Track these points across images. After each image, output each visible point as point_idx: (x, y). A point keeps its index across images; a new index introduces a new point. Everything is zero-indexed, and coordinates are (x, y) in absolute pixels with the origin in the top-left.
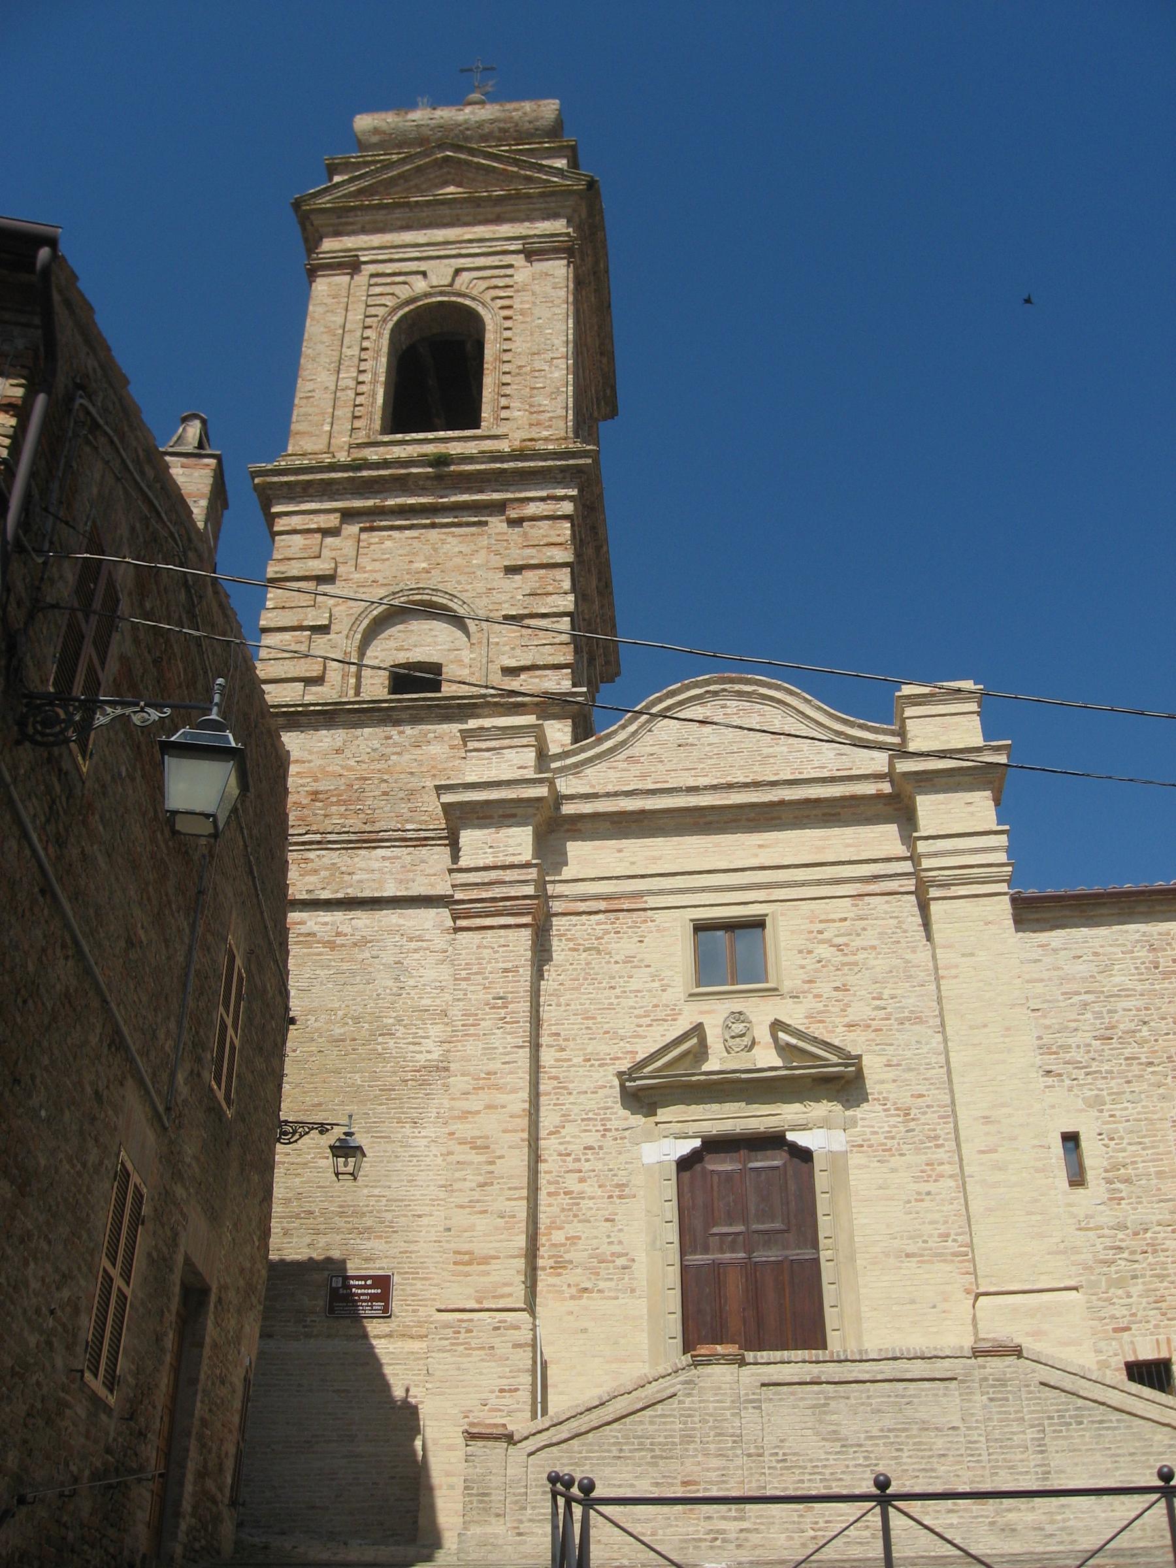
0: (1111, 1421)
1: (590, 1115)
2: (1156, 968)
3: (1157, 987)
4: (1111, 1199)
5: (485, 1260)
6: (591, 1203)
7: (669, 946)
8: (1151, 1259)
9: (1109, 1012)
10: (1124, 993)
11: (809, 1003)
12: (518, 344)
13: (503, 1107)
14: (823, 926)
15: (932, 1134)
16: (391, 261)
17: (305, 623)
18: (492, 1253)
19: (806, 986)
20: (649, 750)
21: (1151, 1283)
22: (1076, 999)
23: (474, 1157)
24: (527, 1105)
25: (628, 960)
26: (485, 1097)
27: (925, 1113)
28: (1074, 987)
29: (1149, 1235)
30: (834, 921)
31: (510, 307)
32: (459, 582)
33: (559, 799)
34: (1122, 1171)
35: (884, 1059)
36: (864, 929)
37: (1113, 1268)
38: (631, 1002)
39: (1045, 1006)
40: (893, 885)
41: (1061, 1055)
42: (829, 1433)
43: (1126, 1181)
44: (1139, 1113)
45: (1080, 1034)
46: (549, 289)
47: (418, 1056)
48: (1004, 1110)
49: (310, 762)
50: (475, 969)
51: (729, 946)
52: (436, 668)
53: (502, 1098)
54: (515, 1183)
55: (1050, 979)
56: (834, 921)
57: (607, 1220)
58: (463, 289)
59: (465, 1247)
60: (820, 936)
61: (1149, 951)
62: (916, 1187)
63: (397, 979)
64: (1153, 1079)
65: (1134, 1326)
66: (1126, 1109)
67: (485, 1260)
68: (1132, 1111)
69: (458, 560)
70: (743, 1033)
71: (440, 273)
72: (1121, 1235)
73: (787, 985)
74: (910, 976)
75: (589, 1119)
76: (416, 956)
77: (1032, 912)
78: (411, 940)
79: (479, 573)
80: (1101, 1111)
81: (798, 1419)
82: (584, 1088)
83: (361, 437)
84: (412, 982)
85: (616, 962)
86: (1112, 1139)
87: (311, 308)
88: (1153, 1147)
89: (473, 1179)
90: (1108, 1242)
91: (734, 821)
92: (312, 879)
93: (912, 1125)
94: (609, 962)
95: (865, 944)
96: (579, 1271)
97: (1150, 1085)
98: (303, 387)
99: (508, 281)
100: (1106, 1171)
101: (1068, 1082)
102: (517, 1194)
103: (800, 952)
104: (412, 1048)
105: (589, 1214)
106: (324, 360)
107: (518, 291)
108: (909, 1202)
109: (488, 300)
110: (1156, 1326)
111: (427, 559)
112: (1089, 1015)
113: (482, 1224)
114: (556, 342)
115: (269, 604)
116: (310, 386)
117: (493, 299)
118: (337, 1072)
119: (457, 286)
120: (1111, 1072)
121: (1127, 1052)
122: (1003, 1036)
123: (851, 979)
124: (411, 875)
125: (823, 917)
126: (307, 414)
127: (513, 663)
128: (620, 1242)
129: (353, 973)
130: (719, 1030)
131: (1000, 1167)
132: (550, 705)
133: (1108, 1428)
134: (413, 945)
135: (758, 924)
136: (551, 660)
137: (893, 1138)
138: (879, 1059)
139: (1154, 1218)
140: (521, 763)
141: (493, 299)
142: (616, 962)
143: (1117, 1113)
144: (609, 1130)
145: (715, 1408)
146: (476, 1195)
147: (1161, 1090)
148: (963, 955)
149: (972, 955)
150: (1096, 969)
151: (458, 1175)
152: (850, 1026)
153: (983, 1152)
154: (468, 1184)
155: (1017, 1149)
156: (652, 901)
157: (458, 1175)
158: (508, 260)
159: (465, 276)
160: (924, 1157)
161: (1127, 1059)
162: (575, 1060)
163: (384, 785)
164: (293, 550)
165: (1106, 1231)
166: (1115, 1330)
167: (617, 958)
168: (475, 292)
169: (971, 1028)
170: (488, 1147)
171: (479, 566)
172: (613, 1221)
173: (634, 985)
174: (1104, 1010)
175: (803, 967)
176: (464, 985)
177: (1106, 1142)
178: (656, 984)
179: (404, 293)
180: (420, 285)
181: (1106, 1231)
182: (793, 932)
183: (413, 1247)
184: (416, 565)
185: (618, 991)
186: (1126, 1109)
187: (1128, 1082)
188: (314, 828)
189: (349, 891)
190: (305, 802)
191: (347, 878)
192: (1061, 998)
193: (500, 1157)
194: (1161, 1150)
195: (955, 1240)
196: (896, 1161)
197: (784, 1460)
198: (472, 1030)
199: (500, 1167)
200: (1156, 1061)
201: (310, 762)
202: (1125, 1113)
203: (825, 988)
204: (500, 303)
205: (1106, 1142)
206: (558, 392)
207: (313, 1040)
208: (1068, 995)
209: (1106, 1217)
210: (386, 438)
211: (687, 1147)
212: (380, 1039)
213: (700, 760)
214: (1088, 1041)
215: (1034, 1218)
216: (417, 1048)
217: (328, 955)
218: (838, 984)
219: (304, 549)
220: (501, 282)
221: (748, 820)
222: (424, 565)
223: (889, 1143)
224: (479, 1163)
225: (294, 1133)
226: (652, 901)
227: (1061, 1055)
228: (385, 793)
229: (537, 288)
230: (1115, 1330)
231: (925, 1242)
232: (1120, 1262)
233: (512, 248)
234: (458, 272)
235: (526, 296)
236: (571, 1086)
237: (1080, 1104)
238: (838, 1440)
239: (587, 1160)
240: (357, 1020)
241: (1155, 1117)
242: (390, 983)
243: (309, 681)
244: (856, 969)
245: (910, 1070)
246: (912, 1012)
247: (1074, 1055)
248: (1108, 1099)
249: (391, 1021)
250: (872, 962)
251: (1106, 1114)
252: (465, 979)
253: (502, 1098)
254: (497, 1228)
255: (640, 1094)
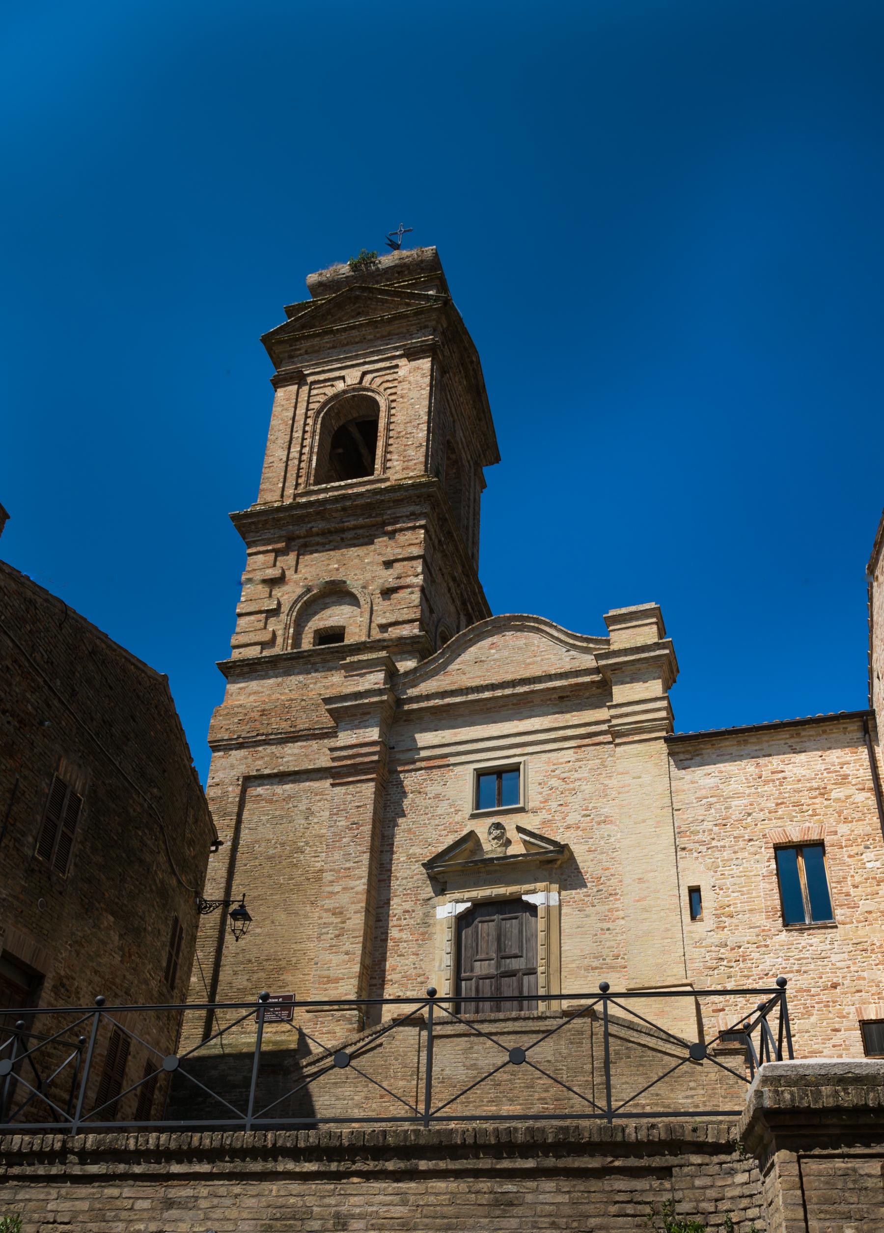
0: (649, 1056)
1: (409, 892)
2: (760, 778)
3: (759, 790)
4: (718, 928)
5: (337, 980)
6: (405, 945)
7: (460, 785)
8: (742, 965)
9: (726, 808)
10: (737, 795)
11: (544, 815)
12: (398, 417)
13: (352, 888)
14: (555, 767)
15: (613, 892)
16: (323, 372)
17: (263, 609)
18: (341, 976)
19: (542, 805)
20: (457, 667)
21: (739, 981)
22: (704, 801)
23: (334, 920)
24: (366, 887)
25: (437, 796)
26: (343, 883)
27: (609, 880)
28: (703, 792)
29: (742, 949)
30: (562, 763)
31: (395, 393)
32: (355, 575)
33: (399, 702)
34: (727, 909)
35: (587, 847)
36: (580, 767)
37: (716, 972)
38: (437, 822)
39: (683, 807)
40: (601, 738)
41: (692, 838)
42: (472, 1065)
43: (729, 916)
44: (741, 872)
45: (705, 823)
46: (419, 378)
47: (317, 864)
48: (652, 874)
49: (262, 692)
50: (342, 807)
51: (498, 786)
52: (343, 628)
53: (352, 883)
54: (356, 934)
55: (689, 790)
56: (562, 763)
57: (414, 954)
58: (368, 385)
59: (326, 973)
60: (553, 774)
61: (756, 767)
62: (600, 925)
63: (307, 818)
64: (752, 850)
65: (727, 1009)
66: (732, 870)
67: (337, 980)
68: (736, 871)
69: (356, 561)
70: (506, 837)
71: (352, 376)
72: (722, 950)
73: (531, 805)
74: (607, 795)
75: (408, 894)
76: (319, 804)
77: (688, 746)
78: (316, 795)
79: (368, 567)
80: (716, 872)
81: (452, 1057)
82: (406, 875)
83: (301, 489)
84: (316, 821)
85: (430, 798)
86: (722, 889)
87: (274, 409)
88: (748, 893)
89: (332, 932)
90: (714, 955)
91: (504, 706)
92: (260, 762)
93: (601, 887)
94: (425, 799)
95: (580, 776)
96: (396, 985)
97: (749, 854)
98: (268, 460)
99: (395, 376)
100: (716, 910)
101: (695, 854)
102: (357, 940)
103: (540, 784)
104: (313, 859)
105: (404, 951)
106: (280, 441)
107: (400, 382)
108: (596, 935)
109: (382, 390)
110: (742, 1008)
111: (338, 562)
112: (713, 811)
113: (336, 959)
114: (422, 413)
115: (243, 599)
116: (271, 459)
117: (385, 389)
118: (270, 876)
119: (364, 384)
120: (725, 847)
121: (735, 833)
122: (655, 827)
123: (570, 799)
124: (317, 756)
125: (555, 762)
126: (268, 478)
127: (384, 621)
128: (421, 968)
129: (282, 817)
130: (486, 835)
131: (645, 910)
132: (404, 646)
133: (646, 1061)
134: (318, 798)
135: (515, 769)
136: (406, 617)
137: (589, 896)
138: (584, 847)
139: (746, 939)
140: (376, 681)
141: (385, 389)
142: (430, 798)
143: (726, 873)
144: (419, 900)
145: (403, 1051)
146: (334, 942)
147: (757, 857)
148: (634, 778)
149: (640, 777)
150: (720, 781)
151: (324, 931)
152: (568, 827)
153: (638, 901)
154: (330, 936)
155: (659, 898)
156: (452, 760)
157: (324, 931)
158: (394, 362)
159: (369, 377)
160: (607, 907)
161: (735, 838)
162: (402, 859)
163: (303, 703)
164: (258, 564)
165: (713, 948)
166: (714, 1011)
167: (429, 796)
168: (374, 386)
169: (635, 823)
170: (342, 913)
171: (368, 563)
172: (418, 955)
173: (439, 811)
174: (723, 807)
175: (541, 793)
176: (335, 817)
177: (718, 891)
178: (453, 810)
179: (330, 392)
180: (340, 386)
181: (713, 948)
182: (536, 772)
183: (307, 977)
184: (331, 567)
185: (430, 815)
186: (732, 870)
187: (735, 852)
188: (261, 732)
189: (281, 768)
190: (257, 717)
191: (280, 760)
192: (694, 801)
193: (348, 919)
194: (754, 895)
195: (623, 958)
196: (589, 910)
197: (443, 1082)
198: (338, 844)
199: (349, 924)
200: (755, 838)
201: (262, 692)
202: (731, 872)
203: (554, 805)
204: (389, 391)
205: (718, 891)
206: (421, 445)
207: (256, 858)
208: (699, 799)
209: (716, 938)
210: (316, 488)
211: (462, 907)
212: (295, 855)
213: (488, 671)
214: (710, 827)
215: (666, 941)
216: (317, 859)
217: (269, 807)
218: (561, 803)
219: (264, 563)
220: (390, 377)
221: (513, 704)
222: (336, 566)
223: (586, 899)
224: (337, 923)
225: (211, 906)
226: (452, 760)
227: (692, 838)
228: (303, 708)
229: (411, 379)
230: (714, 1011)
231: (604, 959)
232: (722, 968)
233: (398, 353)
234: (364, 374)
235: (405, 385)
236: (398, 875)
237: (702, 868)
238: (476, 1069)
239: (405, 919)
240: (283, 844)
241: (752, 874)
242: (303, 822)
243: (264, 645)
244: (574, 792)
245: (602, 853)
246: (606, 817)
247: (700, 837)
248: (721, 864)
249: (302, 844)
250: (583, 788)
251: (719, 873)
252: (337, 814)
253: (352, 883)
254: (344, 961)
255: (438, 876)
